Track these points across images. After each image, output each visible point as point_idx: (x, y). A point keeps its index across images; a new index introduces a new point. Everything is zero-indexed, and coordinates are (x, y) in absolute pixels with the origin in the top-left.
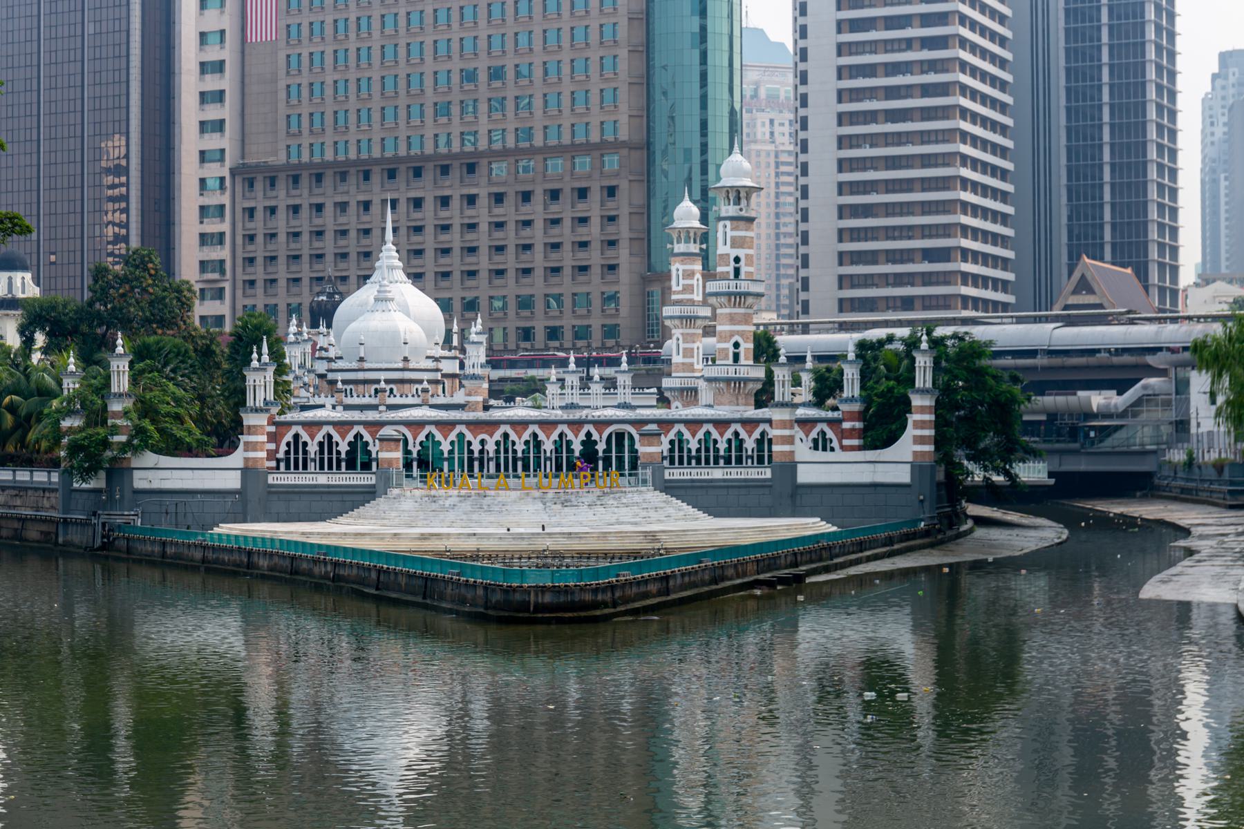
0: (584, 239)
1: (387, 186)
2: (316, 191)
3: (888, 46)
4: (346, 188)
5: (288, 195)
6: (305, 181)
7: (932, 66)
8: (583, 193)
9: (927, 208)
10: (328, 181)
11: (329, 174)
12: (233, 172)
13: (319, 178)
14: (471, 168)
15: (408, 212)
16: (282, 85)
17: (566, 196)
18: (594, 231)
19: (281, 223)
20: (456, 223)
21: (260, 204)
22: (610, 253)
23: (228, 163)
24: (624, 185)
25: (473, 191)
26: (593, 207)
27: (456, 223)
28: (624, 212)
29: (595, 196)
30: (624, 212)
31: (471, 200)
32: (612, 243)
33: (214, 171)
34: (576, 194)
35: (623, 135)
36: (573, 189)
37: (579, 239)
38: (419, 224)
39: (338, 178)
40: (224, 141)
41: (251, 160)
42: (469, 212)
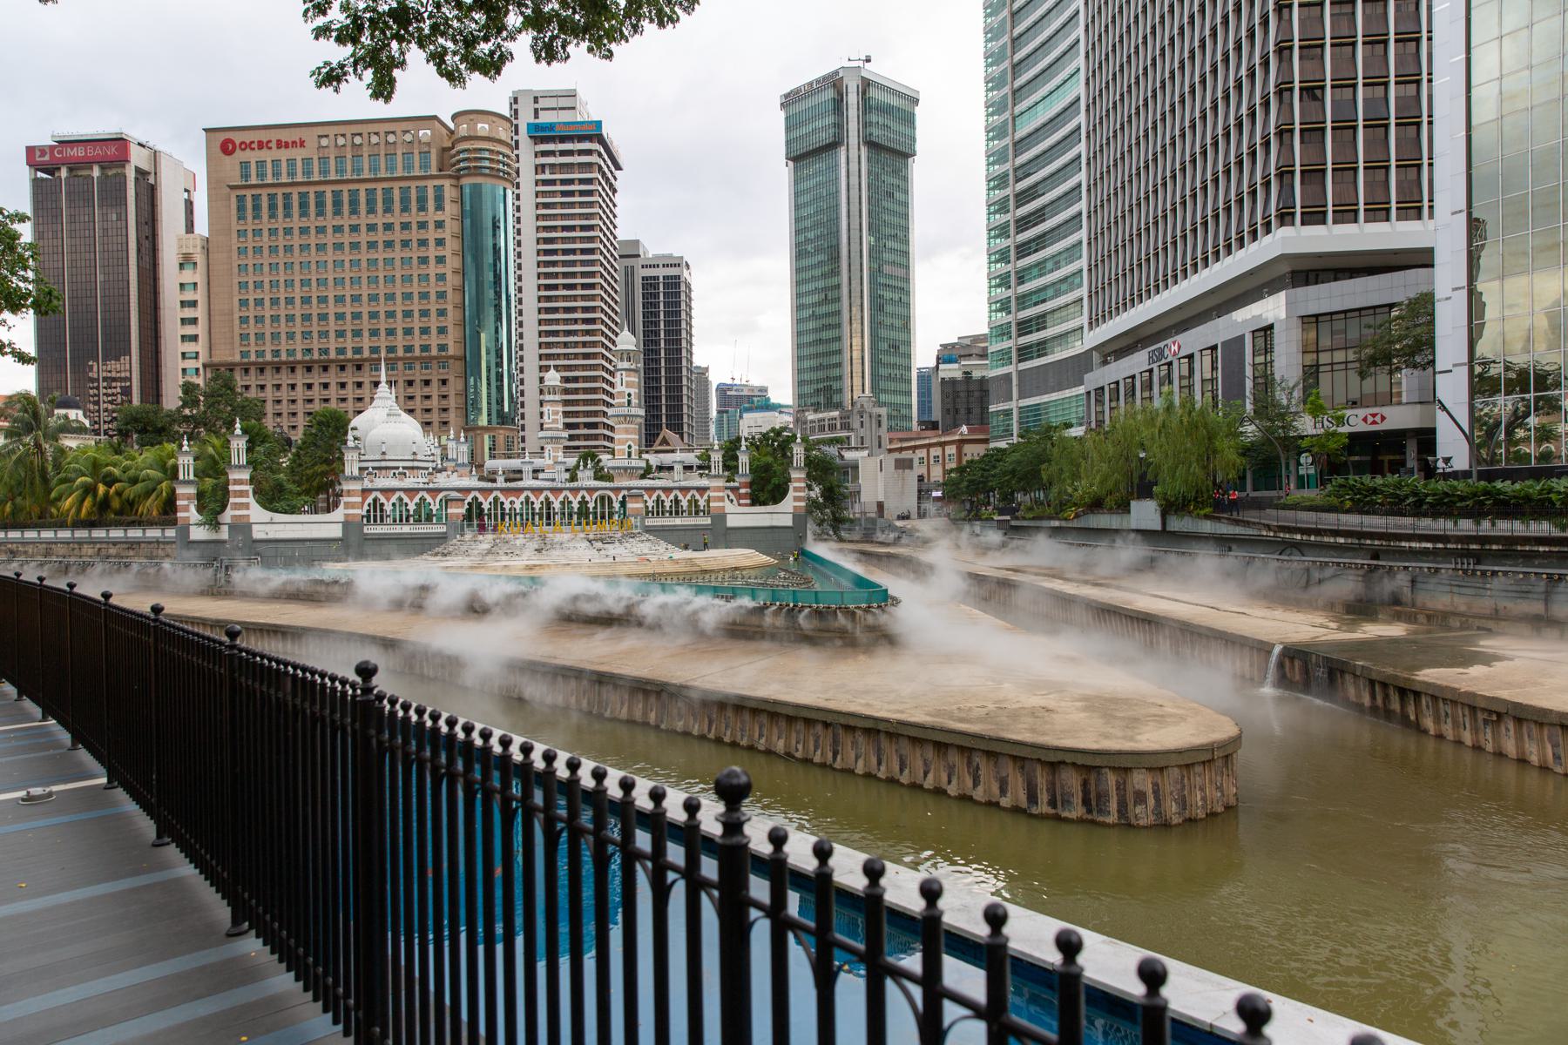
3: (566, 322)
6: (253, 371)
7: (588, 333)
9: (586, 403)
10: (268, 372)
12: (205, 366)
13: (262, 370)
14: (359, 368)
16: (236, 316)
17: (418, 384)
18: (434, 403)
20: (350, 397)
23: (202, 360)
24: (451, 379)
26: (434, 390)
27: (350, 397)
30: (452, 393)
31: (359, 385)
32: (445, 410)
33: (191, 364)
35: (451, 352)
40: (200, 347)
41: (216, 359)
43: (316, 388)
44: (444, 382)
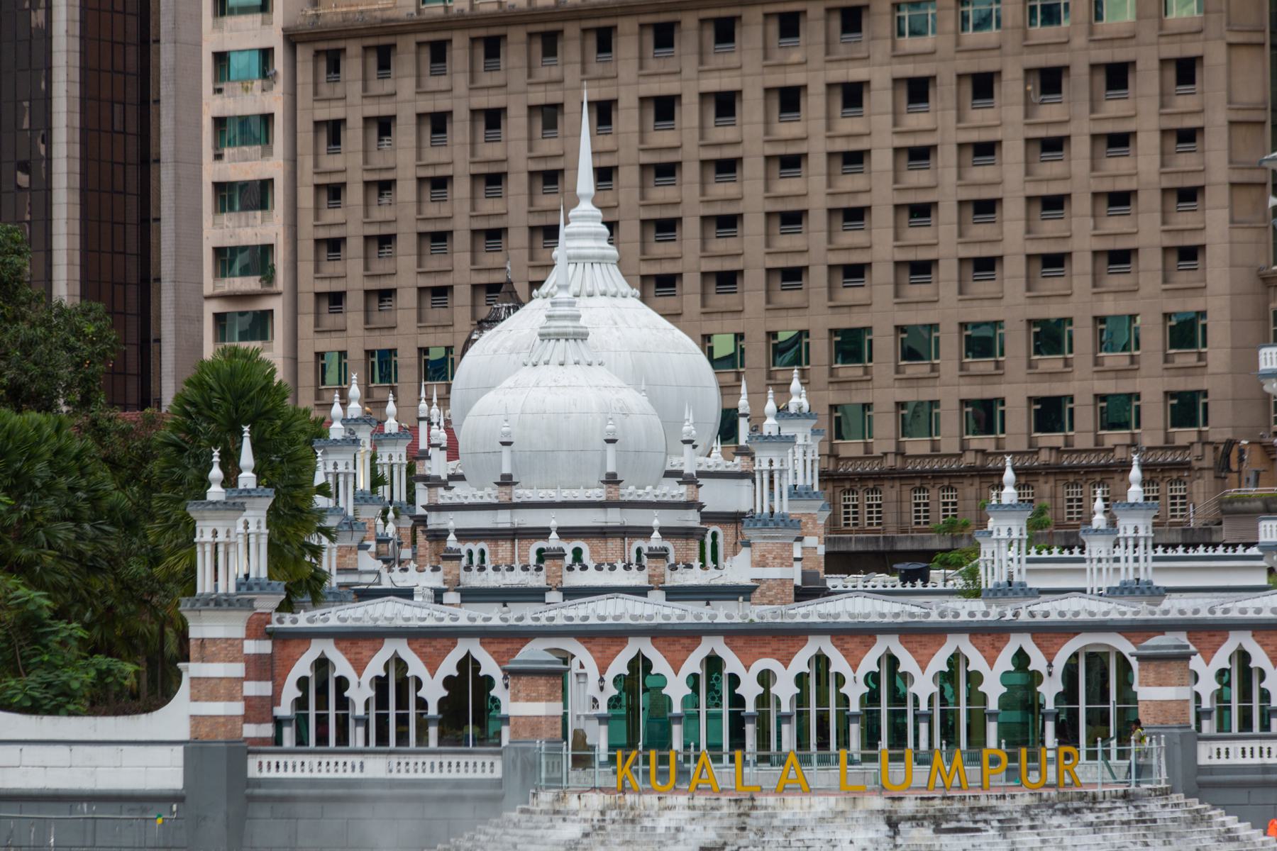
0: (1123, 185)
1: (653, 65)
2: (486, 79)
4: (555, 73)
5: (420, 90)
6: (459, 53)
8: (1117, 76)
10: (515, 54)
11: (516, 36)
12: (293, 39)
13: (493, 48)
15: (702, 127)
17: (1078, 83)
18: (1144, 167)
19: (404, 156)
20: (817, 149)
21: (354, 108)
22: (1184, 219)
24: (1215, 55)
25: (856, 73)
26: (1142, 109)
27: (817, 149)
28: (1216, 121)
29: (1147, 81)
30: (1216, 121)
31: (853, 95)
32: (1189, 195)
34: (1101, 79)
36: (1094, 67)
37: (1107, 186)
38: (728, 153)
39: (538, 47)
42: (847, 125)
43: (689, 113)
44: (1186, 70)
